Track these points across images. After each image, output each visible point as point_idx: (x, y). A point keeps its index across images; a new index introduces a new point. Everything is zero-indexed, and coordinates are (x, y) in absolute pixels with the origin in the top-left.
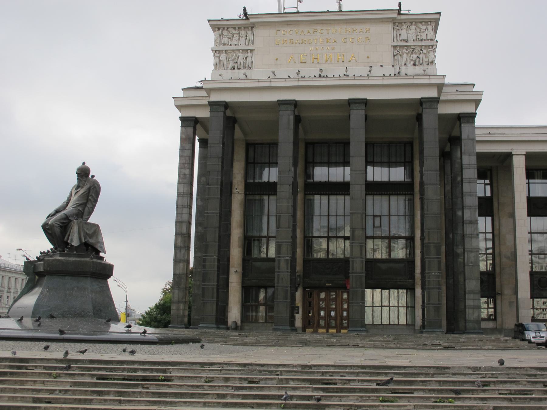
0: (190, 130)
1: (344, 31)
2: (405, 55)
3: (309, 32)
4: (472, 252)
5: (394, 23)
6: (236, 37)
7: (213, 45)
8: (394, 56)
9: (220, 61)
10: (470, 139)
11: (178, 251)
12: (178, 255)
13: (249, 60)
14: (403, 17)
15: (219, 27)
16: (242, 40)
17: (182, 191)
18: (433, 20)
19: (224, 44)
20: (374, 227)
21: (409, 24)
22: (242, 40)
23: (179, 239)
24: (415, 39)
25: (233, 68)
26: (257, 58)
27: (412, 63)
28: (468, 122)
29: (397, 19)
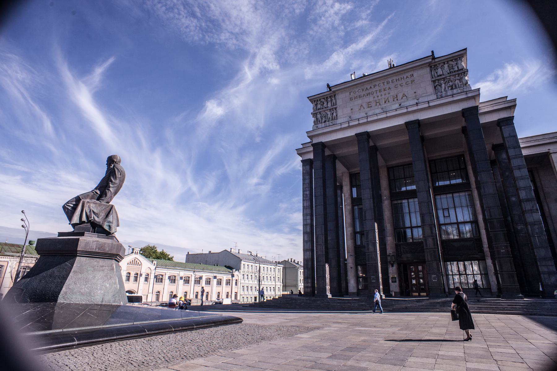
0: (308, 167)
1: (395, 80)
2: (443, 85)
3: (371, 87)
4: (535, 224)
5: (431, 67)
6: (325, 104)
7: (312, 111)
8: (435, 87)
9: (317, 119)
10: (512, 136)
11: (305, 244)
12: (306, 247)
13: (335, 114)
14: (436, 60)
15: (314, 99)
16: (329, 105)
17: (305, 205)
18: (461, 54)
19: (319, 109)
20: (444, 217)
21: (442, 64)
22: (329, 105)
23: (306, 236)
24: (449, 72)
25: (325, 122)
26: (340, 112)
27: (450, 88)
28: (507, 125)
29: (432, 62)
